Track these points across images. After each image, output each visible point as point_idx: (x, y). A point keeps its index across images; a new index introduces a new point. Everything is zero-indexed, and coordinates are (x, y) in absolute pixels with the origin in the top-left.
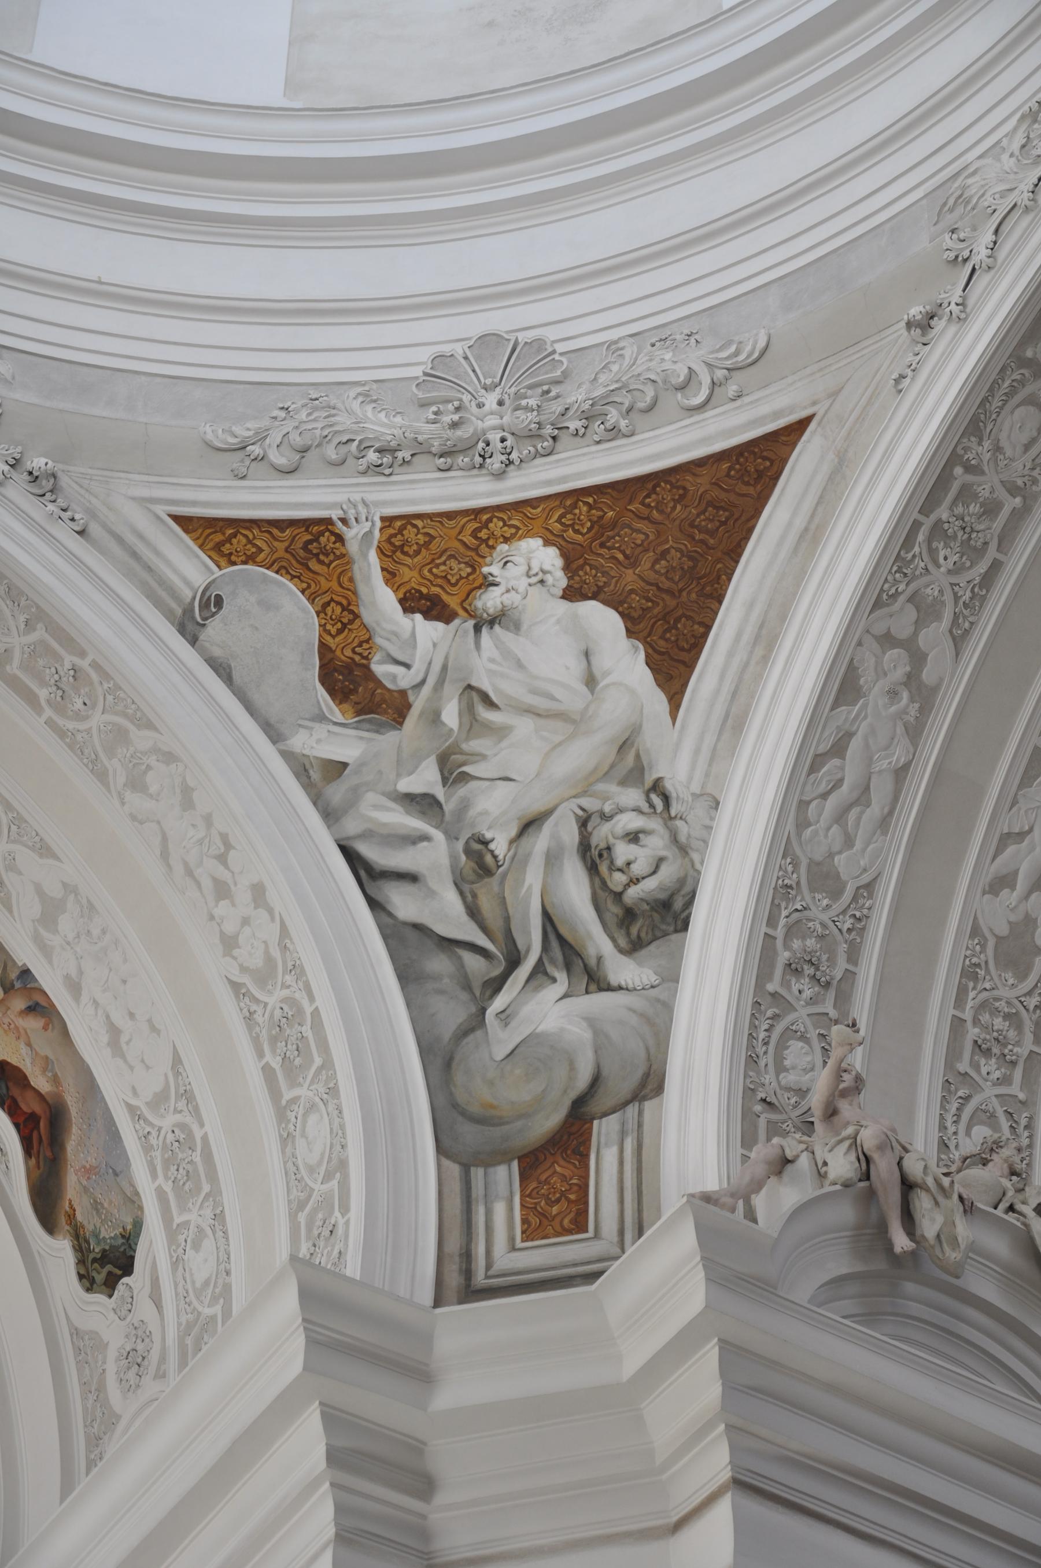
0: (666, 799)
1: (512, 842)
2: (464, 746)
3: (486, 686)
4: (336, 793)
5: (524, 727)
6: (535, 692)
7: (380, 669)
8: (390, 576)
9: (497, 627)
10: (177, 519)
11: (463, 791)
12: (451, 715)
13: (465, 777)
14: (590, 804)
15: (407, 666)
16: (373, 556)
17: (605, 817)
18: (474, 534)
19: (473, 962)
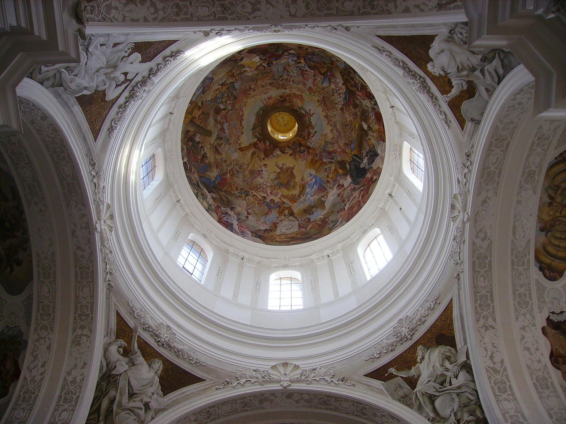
0: (451, 31)
1: (478, 55)
2: (468, 69)
3: (456, 68)
4: (490, 88)
5: (458, 60)
6: (451, 60)
7: (465, 88)
8: (450, 92)
9: (445, 70)
10: (463, 130)
11: (476, 66)
12: (465, 73)
13: (473, 67)
14: (462, 43)
15: (462, 83)
16: (449, 95)
17: (462, 40)
18: (435, 79)
19: (502, 56)
